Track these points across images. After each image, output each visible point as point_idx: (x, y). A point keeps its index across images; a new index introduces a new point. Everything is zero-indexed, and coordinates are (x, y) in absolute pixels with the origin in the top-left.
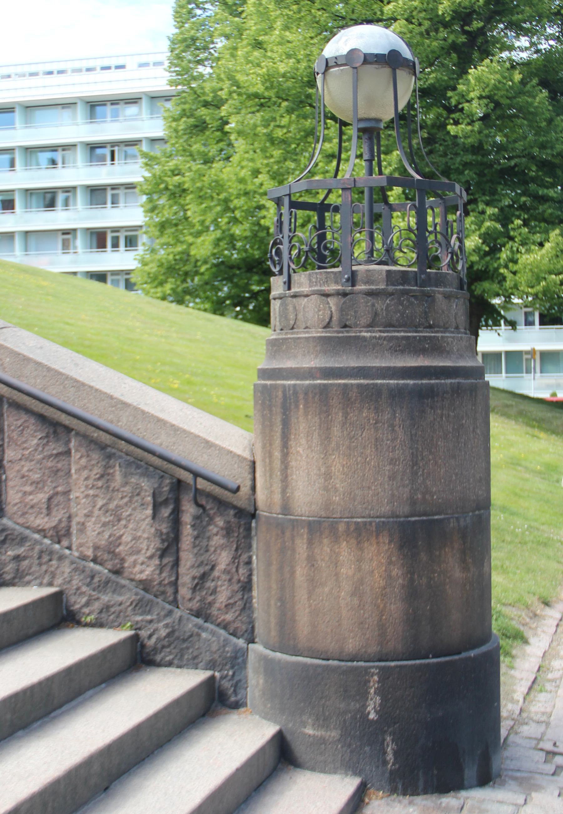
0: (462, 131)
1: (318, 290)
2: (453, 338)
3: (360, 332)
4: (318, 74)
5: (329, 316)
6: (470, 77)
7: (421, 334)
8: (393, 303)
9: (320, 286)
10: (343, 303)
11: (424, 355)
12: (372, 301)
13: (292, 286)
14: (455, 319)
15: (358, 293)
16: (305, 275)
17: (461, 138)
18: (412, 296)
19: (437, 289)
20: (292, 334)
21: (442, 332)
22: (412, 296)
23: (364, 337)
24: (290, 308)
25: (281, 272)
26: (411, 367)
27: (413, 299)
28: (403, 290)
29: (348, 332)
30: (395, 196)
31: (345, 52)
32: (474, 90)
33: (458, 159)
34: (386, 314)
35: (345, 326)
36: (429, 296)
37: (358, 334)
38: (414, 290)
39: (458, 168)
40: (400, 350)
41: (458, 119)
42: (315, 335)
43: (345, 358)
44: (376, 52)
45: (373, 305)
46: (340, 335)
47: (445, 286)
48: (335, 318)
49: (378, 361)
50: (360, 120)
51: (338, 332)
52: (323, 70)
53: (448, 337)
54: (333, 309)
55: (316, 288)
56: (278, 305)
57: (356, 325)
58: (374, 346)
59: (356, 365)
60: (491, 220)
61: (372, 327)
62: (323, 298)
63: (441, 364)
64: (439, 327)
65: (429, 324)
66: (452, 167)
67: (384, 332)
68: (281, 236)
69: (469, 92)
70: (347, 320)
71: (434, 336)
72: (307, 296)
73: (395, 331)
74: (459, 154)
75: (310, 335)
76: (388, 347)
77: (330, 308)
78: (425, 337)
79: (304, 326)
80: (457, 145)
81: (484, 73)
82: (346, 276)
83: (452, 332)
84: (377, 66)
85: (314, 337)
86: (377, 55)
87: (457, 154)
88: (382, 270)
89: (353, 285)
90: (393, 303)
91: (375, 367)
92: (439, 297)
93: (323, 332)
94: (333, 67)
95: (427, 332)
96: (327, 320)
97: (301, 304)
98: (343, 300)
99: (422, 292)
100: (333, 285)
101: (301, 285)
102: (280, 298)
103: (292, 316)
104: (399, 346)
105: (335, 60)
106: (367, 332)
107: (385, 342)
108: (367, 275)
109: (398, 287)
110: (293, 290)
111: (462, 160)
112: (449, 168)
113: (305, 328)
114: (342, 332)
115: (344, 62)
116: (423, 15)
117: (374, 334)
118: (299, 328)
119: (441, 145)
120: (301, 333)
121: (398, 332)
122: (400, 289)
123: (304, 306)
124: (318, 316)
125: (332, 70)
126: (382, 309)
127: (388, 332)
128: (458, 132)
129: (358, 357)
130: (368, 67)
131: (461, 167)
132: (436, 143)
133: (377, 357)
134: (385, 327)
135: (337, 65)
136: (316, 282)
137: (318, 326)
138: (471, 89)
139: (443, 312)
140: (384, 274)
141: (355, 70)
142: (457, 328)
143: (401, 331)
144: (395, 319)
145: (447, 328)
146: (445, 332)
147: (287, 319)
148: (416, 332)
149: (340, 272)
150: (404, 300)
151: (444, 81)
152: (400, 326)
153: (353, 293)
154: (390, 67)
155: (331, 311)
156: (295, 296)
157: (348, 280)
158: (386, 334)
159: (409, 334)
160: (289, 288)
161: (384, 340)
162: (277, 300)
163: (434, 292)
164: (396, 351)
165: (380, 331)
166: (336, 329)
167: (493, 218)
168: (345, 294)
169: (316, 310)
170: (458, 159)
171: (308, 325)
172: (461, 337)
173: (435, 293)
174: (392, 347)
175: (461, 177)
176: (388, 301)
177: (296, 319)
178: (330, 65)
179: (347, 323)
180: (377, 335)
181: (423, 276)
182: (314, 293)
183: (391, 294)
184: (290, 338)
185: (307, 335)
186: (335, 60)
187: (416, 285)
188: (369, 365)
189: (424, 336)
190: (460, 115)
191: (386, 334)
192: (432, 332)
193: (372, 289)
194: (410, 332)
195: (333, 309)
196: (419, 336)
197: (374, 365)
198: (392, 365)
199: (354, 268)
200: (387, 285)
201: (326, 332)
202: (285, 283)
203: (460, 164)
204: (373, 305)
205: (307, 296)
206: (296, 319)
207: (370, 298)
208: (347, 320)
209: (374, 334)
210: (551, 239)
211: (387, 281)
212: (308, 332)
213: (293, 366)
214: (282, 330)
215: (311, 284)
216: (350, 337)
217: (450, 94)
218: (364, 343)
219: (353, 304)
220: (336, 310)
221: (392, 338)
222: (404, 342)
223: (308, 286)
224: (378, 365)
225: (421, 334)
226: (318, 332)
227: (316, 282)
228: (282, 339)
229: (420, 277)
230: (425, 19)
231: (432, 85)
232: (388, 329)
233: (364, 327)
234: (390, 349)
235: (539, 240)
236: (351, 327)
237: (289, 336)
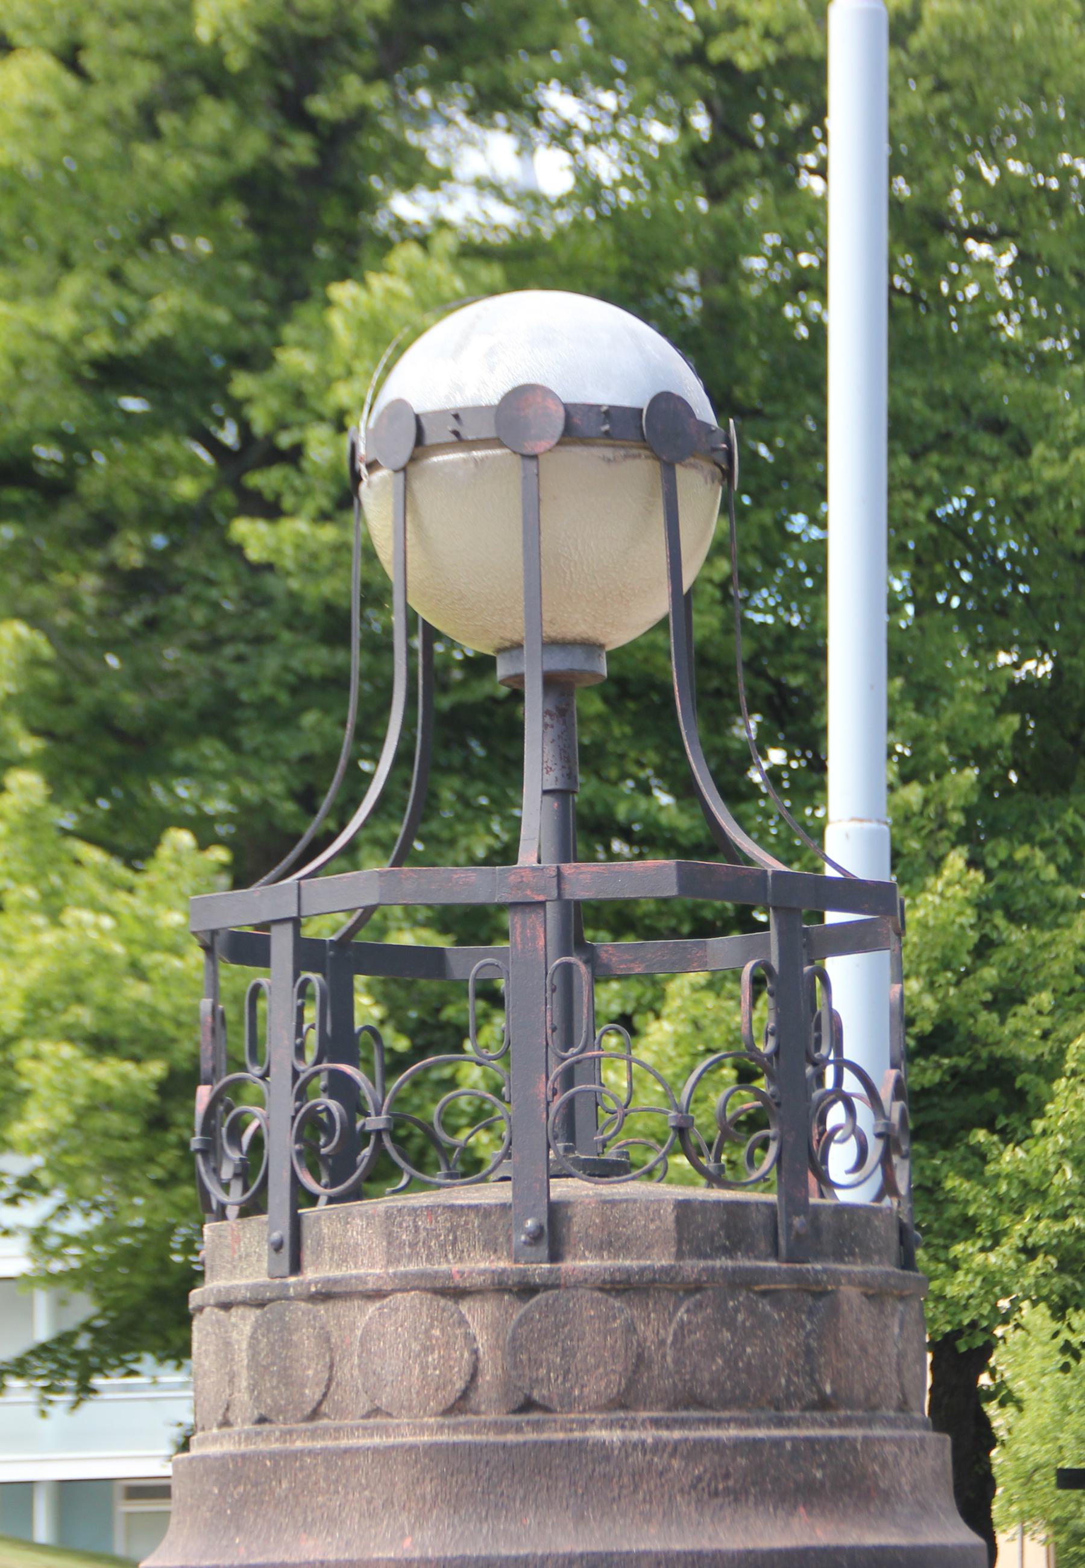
0: (298, 547)
1: (422, 1275)
2: (898, 1442)
3: (585, 1425)
4: (372, 466)
5: (466, 1369)
6: (336, 320)
7: (795, 1432)
8: (699, 1318)
9: (429, 1258)
10: (520, 1323)
11: (809, 1505)
12: (628, 1312)
13: (307, 1256)
14: (899, 1373)
15: (575, 1286)
16: (369, 1218)
17: (288, 574)
18: (764, 1294)
19: (842, 1267)
20: (314, 1435)
21: (861, 1423)
22: (764, 1294)
23: (602, 1444)
24: (306, 1339)
25: (254, 1207)
26: (771, 1553)
27: (765, 1306)
28: (734, 1271)
29: (537, 1426)
30: (14, 817)
31: (492, 396)
32: (350, 373)
33: (272, 664)
34: (677, 1362)
35: (528, 1405)
36: (821, 1294)
37: (577, 1435)
38: (772, 1271)
39: (271, 701)
40: (727, 1491)
41: (278, 496)
42: (410, 1439)
43: (531, 1520)
44: (605, 398)
45: (630, 1328)
46: (511, 1438)
47: (867, 1258)
48: (487, 1377)
49: (653, 1531)
50: (553, 644)
51: (500, 1427)
52: (402, 459)
53: (883, 1440)
54: (482, 1342)
55: (412, 1267)
56: (247, 1330)
57: (569, 1403)
58: (637, 1476)
59: (579, 1549)
60: (416, 924)
61: (624, 1407)
62: (442, 1302)
63: (871, 1539)
64: (851, 1404)
65: (821, 1392)
66: (245, 696)
67: (668, 1425)
68: (257, 1070)
69: (328, 382)
70: (536, 1382)
71: (842, 1439)
72: (378, 1295)
73: (706, 1422)
74: (272, 639)
75: (391, 1441)
76: (686, 1481)
77: (470, 1339)
78: (810, 1441)
79: (365, 1405)
80: (267, 601)
81: (398, 307)
82: (530, 1223)
83: (892, 1423)
84: (609, 453)
85: (412, 1448)
86: (611, 414)
87: (260, 640)
88: (660, 1201)
89: (555, 1257)
90: (699, 1318)
91: (646, 1554)
92: (850, 1293)
93: (441, 1428)
94: (442, 447)
95: (814, 1423)
96: (460, 1385)
97: (352, 1327)
98: (519, 1310)
99: (799, 1277)
100: (477, 1254)
101: (346, 1253)
102: (261, 1304)
103: (312, 1372)
104: (727, 1476)
105: (453, 425)
106: (610, 1425)
107: (676, 1463)
108: (605, 1222)
109: (718, 1263)
110: (311, 1274)
111: (287, 669)
112: (230, 700)
113: (367, 1416)
114: (519, 1429)
115: (489, 432)
116: (127, 35)
117: (635, 1435)
118: (340, 1412)
119: (196, 599)
120: (351, 1431)
121: (719, 1423)
122: (725, 1271)
123: (367, 1331)
124: (424, 1368)
125: (437, 459)
126: (662, 1343)
127: (683, 1423)
128: (278, 551)
129: (580, 1518)
130: (577, 454)
131: (284, 698)
132: (177, 589)
133: (647, 1518)
134: (674, 1406)
135: (459, 441)
136: (413, 1245)
137: (424, 1407)
138: (337, 369)
139: (863, 1349)
140: (669, 1215)
141: (532, 465)
142: (903, 1406)
143: (729, 1421)
144: (707, 1376)
145: (874, 1408)
146: (868, 1423)
147: (286, 1377)
148: (780, 1423)
149: (504, 1207)
150: (736, 1310)
151: (217, 327)
152: (726, 1405)
153: (557, 1286)
154: (657, 458)
155: (475, 1352)
156: (325, 1295)
157: (535, 1238)
158: (677, 1434)
159: (760, 1433)
160: (296, 1267)
161: (673, 1454)
162: (236, 1313)
163: (834, 1275)
164: (716, 1494)
165: (656, 1423)
166: (492, 1417)
167: (422, 914)
168: (526, 1290)
169: (416, 1347)
170: (272, 664)
171: (383, 1401)
172: (922, 1440)
173: (838, 1283)
174: (699, 1479)
175: (282, 737)
176: (682, 1314)
177: (330, 1380)
178: (430, 439)
179: (536, 1395)
180: (649, 1435)
181: (797, 1221)
182: (407, 1284)
183: (696, 1288)
184: (311, 1452)
185: (377, 1440)
186: (453, 425)
187: (775, 1254)
188: (626, 1547)
189: (808, 1440)
190: (285, 479)
191: (677, 1434)
192: (832, 1424)
193: (628, 1271)
194: (758, 1424)
195: (482, 1342)
196: (794, 1440)
197: (642, 1547)
198: (706, 1544)
199: (560, 1189)
200: (680, 1255)
201: (455, 1429)
202: (278, 1247)
203: (278, 682)
204: (630, 1328)
205: (378, 1295)
206: (330, 1380)
207: (617, 1304)
208: (536, 1382)
209: (635, 1435)
210: (672, 1005)
211: (679, 1242)
212: (384, 1430)
213: (331, 1557)
214: (262, 1420)
215: (393, 1251)
216: (550, 1444)
217: (242, 384)
218: (600, 1469)
219: (558, 1326)
220: (493, 1348)
221: (701, 1446)
222: (742, 1461)
223: (379, 1256)
224: (657, 1546)
225: (795, 1432)
226: (423, 1428)
227: (413, 1245)
228: (273, 1455)
229: (790, 1226)
230: (133, 53)
231: (162, 348)
232: (684, 1414)
233: (597, 1408)
234: (694, 1487)
235: (615, 1008)
236: (547, 1409)
237: (299, 1444)
